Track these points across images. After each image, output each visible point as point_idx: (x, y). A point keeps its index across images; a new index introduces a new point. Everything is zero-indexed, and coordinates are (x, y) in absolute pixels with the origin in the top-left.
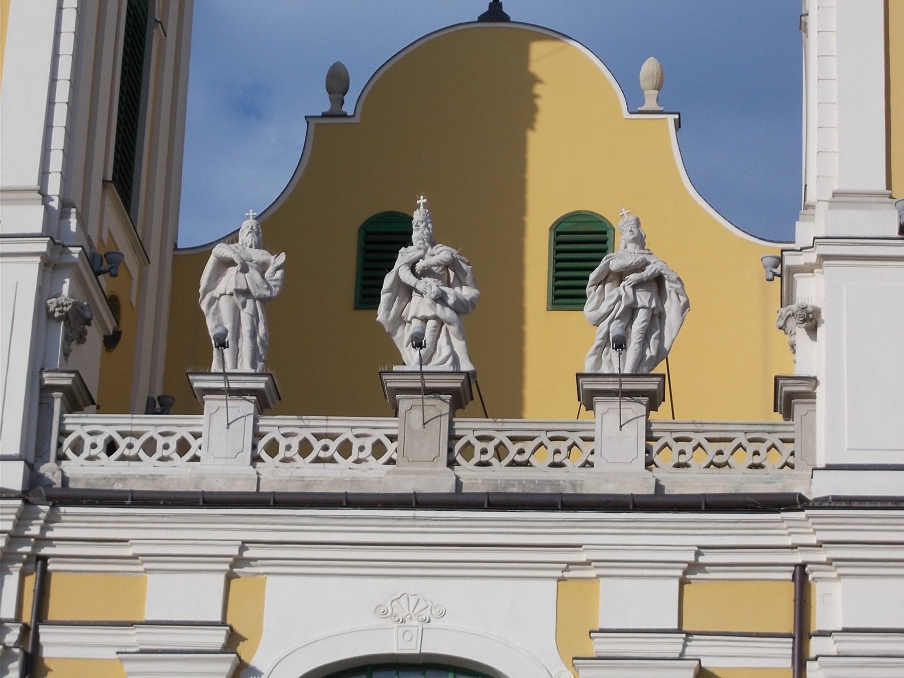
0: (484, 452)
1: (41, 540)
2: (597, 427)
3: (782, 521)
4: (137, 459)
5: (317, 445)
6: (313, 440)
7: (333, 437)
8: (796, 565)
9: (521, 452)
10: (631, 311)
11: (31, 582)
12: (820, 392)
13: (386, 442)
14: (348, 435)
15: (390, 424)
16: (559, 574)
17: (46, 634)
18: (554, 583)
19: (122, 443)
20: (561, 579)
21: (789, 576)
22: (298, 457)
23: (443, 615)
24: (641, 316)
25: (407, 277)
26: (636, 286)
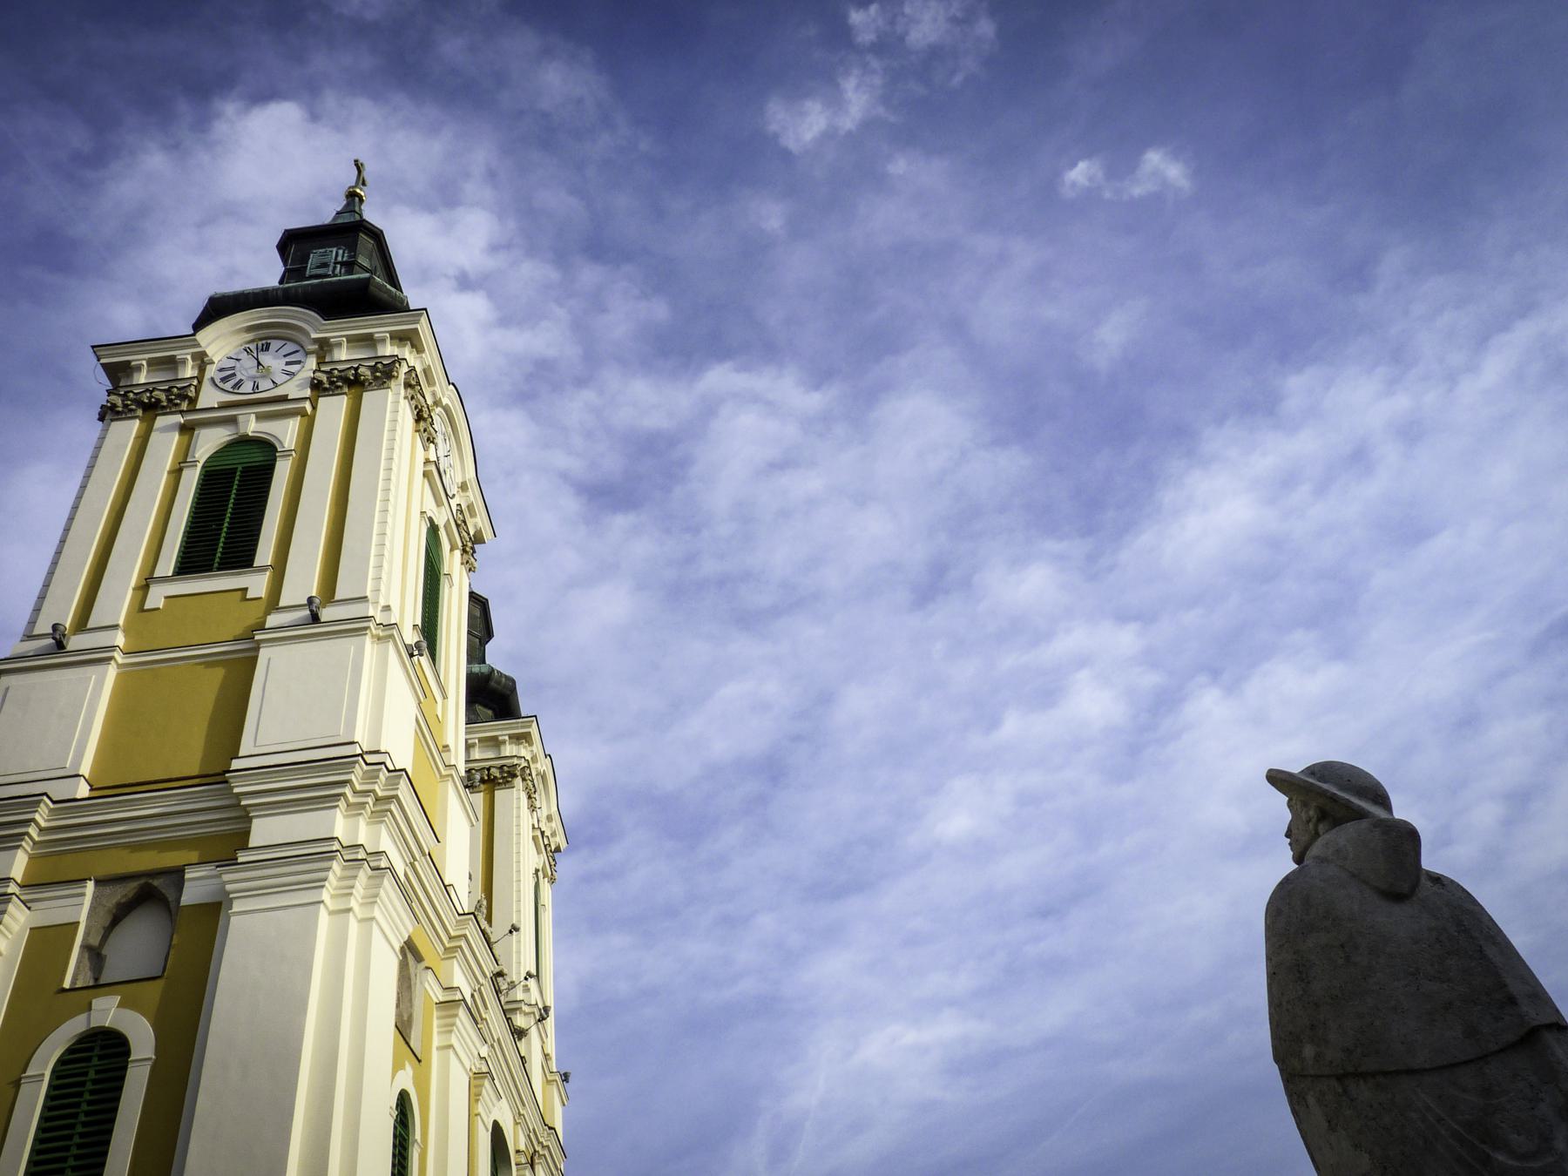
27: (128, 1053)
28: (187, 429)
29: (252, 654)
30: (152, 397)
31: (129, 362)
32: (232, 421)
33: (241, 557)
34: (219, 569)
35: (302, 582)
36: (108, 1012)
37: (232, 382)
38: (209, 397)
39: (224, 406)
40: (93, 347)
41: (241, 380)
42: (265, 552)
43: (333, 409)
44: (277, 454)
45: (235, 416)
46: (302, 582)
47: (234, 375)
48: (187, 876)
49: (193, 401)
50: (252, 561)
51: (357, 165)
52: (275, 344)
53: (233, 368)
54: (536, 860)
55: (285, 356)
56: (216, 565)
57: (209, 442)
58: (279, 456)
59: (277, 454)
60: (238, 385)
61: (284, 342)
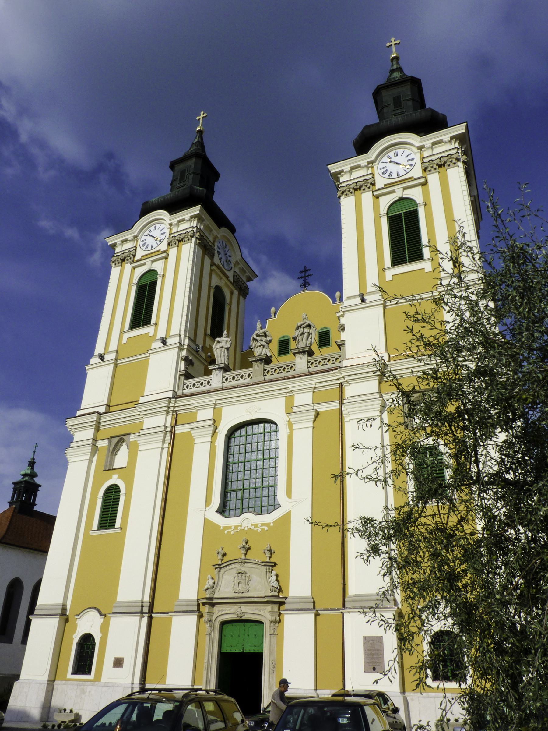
0: (272, 372)
1: (175, 407)
2: (296, 362)
3: (334, 373)
4: (199, 387)
5: (236, 377)
6: (235, 376)
7: (239, 375)
8: (340, 383)
9: (280, 370)
10: (303, 334)
11: (175, 416)
12: (346, 343)
13: (251, 373)
14: (243, 374)
15: (251, 369)
16: (285, 395)
17: (177, 428)
18: (285, 398)
19: (196, 384)
20: (286, 396)
21: (338, 386)
22: (232, 381)
23: (260, 409)
24: (306, 334)
25: (255, 337)
26: (304, 328)
28: (134, 268)
33: (147, 322)
34: (143, 325)
47: (146, 243)
61: (160, 224)
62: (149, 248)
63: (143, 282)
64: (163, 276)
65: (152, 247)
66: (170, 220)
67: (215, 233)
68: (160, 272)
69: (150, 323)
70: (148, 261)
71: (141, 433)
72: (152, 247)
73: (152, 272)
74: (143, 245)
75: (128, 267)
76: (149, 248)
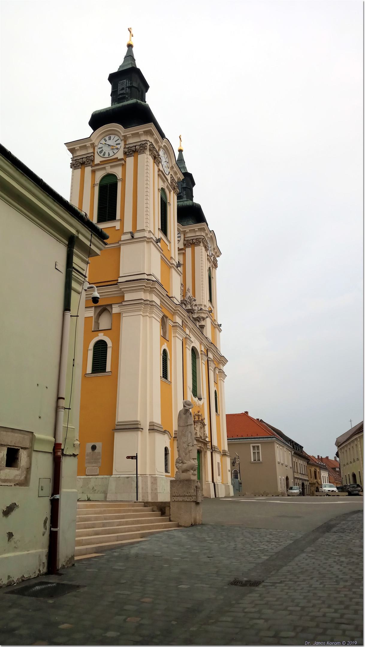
27: (107, 345)
29: (119, 247)
30: (83, 161)
31: (75, 148)
32: (104, 168)
35: (128, 228)
36: (101, 336)
37: (102, 153)
38: (98, 160)
39: (103, 163)
40: (65, 144)
41: (105, 152)
42: (118, 216)
43: (130, 161)
44: (118, 180)
45: (105, 167)
46: (128, 228)
47: (102, 150)
48: (113, 307)
49: (93, 161)
50: (116, 218)
51: (129, 30)
52: (112, 137)
53: (102, 148)
54: (209, 264)
55: (115, 141)
56: (107, 220)
57: (99, 175)
58: (114, 307)
59: (118, 180)
60: (104, 154)
62: (107, 155)
63: (104, 182)
64: (123, 180)
65: (109, 154)
66: (124, 133)
67: (160, 144)
68: (119, 176)
69: (116, 220)
70: (108, 167)
71: (123, 304)
72: (109, 154)
73: (113, 176)
74: (101, 152)
75: (88, 170)
76: (107, 155)
